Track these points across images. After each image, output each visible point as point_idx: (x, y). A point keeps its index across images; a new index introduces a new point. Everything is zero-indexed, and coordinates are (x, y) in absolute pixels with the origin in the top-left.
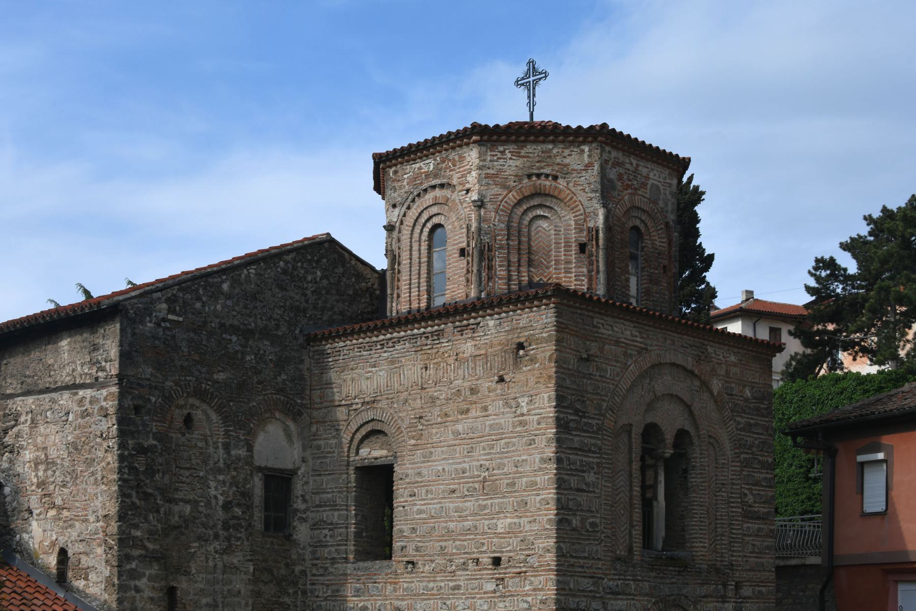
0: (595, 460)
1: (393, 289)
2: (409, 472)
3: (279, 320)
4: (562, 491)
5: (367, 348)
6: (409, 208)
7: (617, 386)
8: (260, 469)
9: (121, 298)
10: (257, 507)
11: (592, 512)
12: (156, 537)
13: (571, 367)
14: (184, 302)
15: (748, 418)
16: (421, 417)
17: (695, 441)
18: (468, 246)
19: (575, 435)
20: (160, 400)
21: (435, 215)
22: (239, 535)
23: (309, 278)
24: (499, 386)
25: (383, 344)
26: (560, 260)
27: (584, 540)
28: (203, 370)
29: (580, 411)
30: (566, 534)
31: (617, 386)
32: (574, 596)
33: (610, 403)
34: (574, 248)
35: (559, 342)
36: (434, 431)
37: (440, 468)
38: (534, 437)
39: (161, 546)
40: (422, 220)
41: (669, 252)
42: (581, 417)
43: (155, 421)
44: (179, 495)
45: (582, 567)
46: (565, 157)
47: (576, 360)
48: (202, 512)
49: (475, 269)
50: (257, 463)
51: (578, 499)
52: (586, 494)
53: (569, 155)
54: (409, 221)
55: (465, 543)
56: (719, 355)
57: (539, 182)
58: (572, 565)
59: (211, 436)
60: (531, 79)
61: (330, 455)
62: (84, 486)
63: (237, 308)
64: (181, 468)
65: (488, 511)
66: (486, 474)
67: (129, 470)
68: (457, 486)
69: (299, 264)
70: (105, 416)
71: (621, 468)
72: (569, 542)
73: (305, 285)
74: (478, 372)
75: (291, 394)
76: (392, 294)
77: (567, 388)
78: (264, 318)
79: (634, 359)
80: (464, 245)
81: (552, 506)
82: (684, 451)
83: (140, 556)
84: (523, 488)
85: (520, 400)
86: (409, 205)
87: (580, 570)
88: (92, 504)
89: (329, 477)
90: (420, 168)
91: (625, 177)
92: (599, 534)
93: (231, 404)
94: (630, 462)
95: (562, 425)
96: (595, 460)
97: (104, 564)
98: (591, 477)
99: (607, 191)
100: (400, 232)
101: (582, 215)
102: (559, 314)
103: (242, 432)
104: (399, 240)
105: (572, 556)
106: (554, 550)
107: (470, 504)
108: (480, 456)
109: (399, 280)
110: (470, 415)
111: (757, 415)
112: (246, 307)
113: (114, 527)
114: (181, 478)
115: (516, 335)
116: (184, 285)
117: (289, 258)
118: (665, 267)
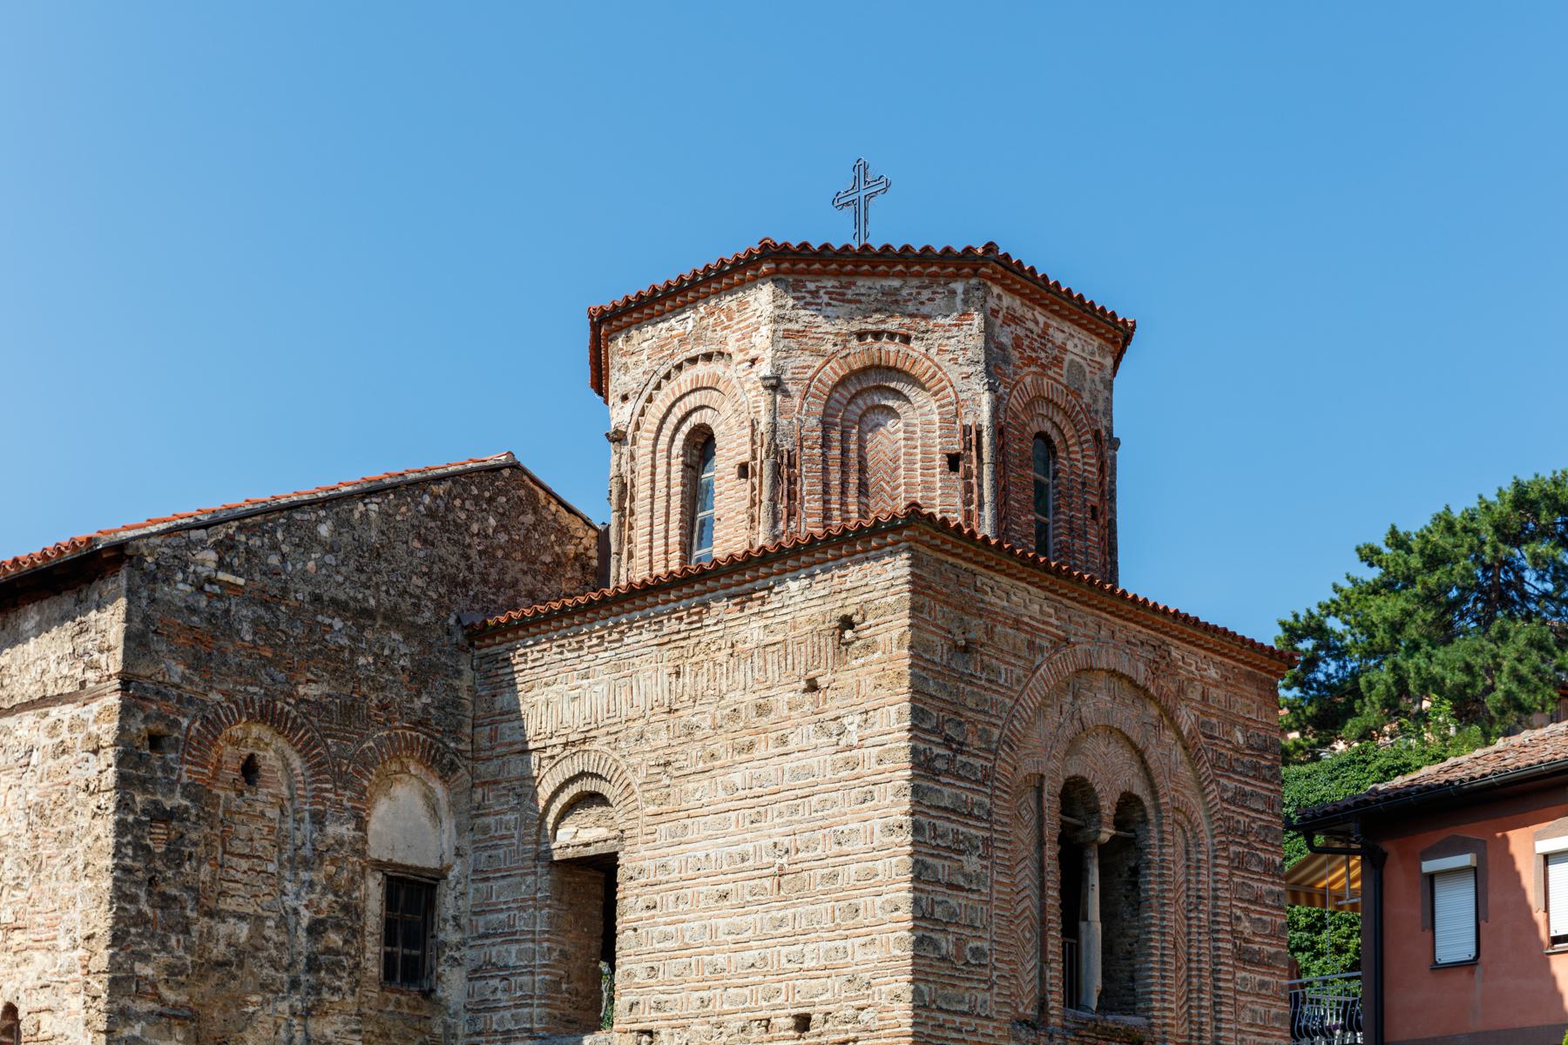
0: (981, 833)
1: (620, 543)
2: (645, 864)
3: (418, 598)
4: (922, 886)
5: (575, 645)
6: (650, 400)
7: (1017, 700)
8: (379, 865)
9: (130, 534)
10: (372, 934)
11: (976, 928)
12: (182, 978)
13: (937, 659)
14: (248, 550)
15: (1240, 781)
16: (667, 764)
17: (1151, 814)
18: (754, 458)
19: (945, 784)
20: (197, 724)
21: (696, 409)
22: (338, 983)
23: (475, 528)
24: (809, 697)
25: (602, 637)
26: (913, 484)
28: (281, 677)
29: (952, 740)
30: (931, 966)
31: (1017, 700)
33: (1006, 731)
34: (939, 461)
35: (915, 610)
36: (691, 786)
37: (701, 854)
38: (871, 787)
39: (191, 997)
40: (673, 420)
41: (1101, 484)
42: (956, 751)
43: (187, 762)
44: (228, 904)
45: (959, 1031)
46: (922, 303)
48: (270, 939)
49: (765, 496)
50: (373, 854)
52: (964, 894)
53: (929, 300)
54: (651, 422)
55: (746, 991)
56: (1191, 665)
57: (877, 346)
58: (940, 1026)
59: (291, 799)
60: (862, 194)
61: (505, 842)
62: (53, 883)
63: (343, 569)
64: (232, 854)
65: (788, 929)
66: (785, 860)
67: (134, 849)
68: (731, 886)
69: (458, 502)
70: (95, 752)
71: (1025, 853)
72: (935, 982)
73: (468, 540)
74: (770, 674)
75: (438, 731)
76: (619, 554)
77: (932, 697)
78: (392, 592)
79: (1046, 655)
80: (746, 457)
81: (905, 913)
82: (1132, 835)
83: (152, 1012)
84: (852, 882)
85: (845, 721)
86: (651, 395)
87: (954, 1035)
88: (65, 917)
89: (502, 883)
90: (670, 329)
91: (1026, 342)
93: (329, 741)
94: (1041, 844)
95: (922, 764)
96: (981, 833)
97: (81, 1027)
98: (972, 864)
99: (996, 364)
100: (634, 442)
101: (951, 404)
102: (915, 562)
103: (348, 793)
104: (633, 458)
105: (940, 1009)
106: (908, 996)
107: (755, 919)
108: (774, 829)
109: (631, 528)
110: (756, 754)
111: (1254, 777)
112: (360, 570)
113: (102, 959)
114: (232, 872)
115: (839, 604)
116: (248, 520)
117: (440, 489)
118: (1094, 509)
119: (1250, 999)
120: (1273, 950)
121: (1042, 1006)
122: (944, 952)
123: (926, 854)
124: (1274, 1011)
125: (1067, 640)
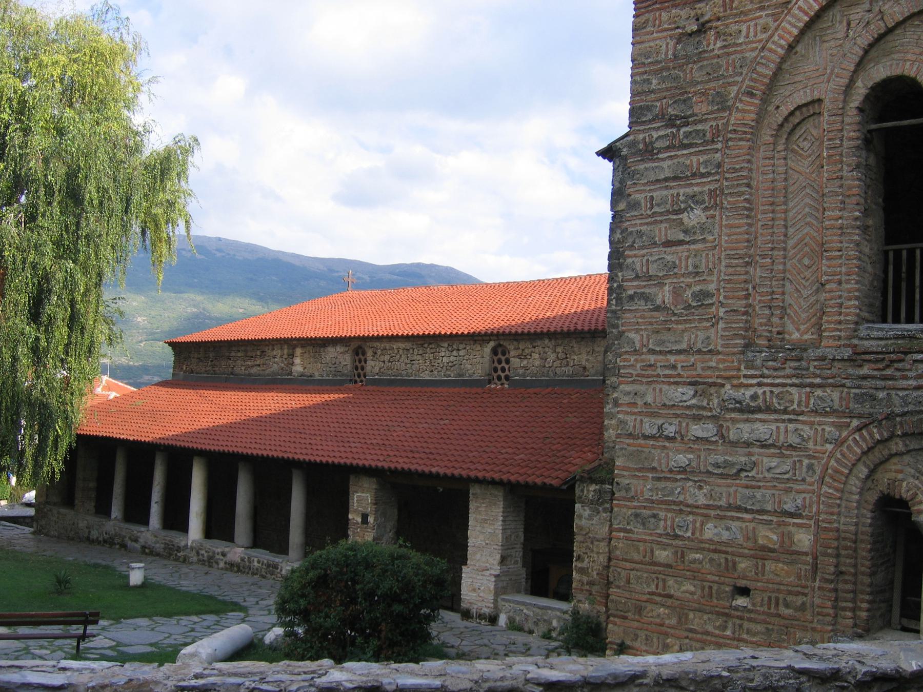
7: (763, 48)
11: (697, 273)
19: (663, 160)
27: (678, 322)
30: (643, 317)
32: (653, 415)
45: (674, 367)
47: (672, 43)
51: (669, 258)
58: (650, 366)
87: (667, 372)
92: (714, 309)
96: (706, 188)
98: (695, 217)
105: (652, 352)
121: (819, 328)
122: (659, 302)
123: (641, 224)
125: (105, 139)
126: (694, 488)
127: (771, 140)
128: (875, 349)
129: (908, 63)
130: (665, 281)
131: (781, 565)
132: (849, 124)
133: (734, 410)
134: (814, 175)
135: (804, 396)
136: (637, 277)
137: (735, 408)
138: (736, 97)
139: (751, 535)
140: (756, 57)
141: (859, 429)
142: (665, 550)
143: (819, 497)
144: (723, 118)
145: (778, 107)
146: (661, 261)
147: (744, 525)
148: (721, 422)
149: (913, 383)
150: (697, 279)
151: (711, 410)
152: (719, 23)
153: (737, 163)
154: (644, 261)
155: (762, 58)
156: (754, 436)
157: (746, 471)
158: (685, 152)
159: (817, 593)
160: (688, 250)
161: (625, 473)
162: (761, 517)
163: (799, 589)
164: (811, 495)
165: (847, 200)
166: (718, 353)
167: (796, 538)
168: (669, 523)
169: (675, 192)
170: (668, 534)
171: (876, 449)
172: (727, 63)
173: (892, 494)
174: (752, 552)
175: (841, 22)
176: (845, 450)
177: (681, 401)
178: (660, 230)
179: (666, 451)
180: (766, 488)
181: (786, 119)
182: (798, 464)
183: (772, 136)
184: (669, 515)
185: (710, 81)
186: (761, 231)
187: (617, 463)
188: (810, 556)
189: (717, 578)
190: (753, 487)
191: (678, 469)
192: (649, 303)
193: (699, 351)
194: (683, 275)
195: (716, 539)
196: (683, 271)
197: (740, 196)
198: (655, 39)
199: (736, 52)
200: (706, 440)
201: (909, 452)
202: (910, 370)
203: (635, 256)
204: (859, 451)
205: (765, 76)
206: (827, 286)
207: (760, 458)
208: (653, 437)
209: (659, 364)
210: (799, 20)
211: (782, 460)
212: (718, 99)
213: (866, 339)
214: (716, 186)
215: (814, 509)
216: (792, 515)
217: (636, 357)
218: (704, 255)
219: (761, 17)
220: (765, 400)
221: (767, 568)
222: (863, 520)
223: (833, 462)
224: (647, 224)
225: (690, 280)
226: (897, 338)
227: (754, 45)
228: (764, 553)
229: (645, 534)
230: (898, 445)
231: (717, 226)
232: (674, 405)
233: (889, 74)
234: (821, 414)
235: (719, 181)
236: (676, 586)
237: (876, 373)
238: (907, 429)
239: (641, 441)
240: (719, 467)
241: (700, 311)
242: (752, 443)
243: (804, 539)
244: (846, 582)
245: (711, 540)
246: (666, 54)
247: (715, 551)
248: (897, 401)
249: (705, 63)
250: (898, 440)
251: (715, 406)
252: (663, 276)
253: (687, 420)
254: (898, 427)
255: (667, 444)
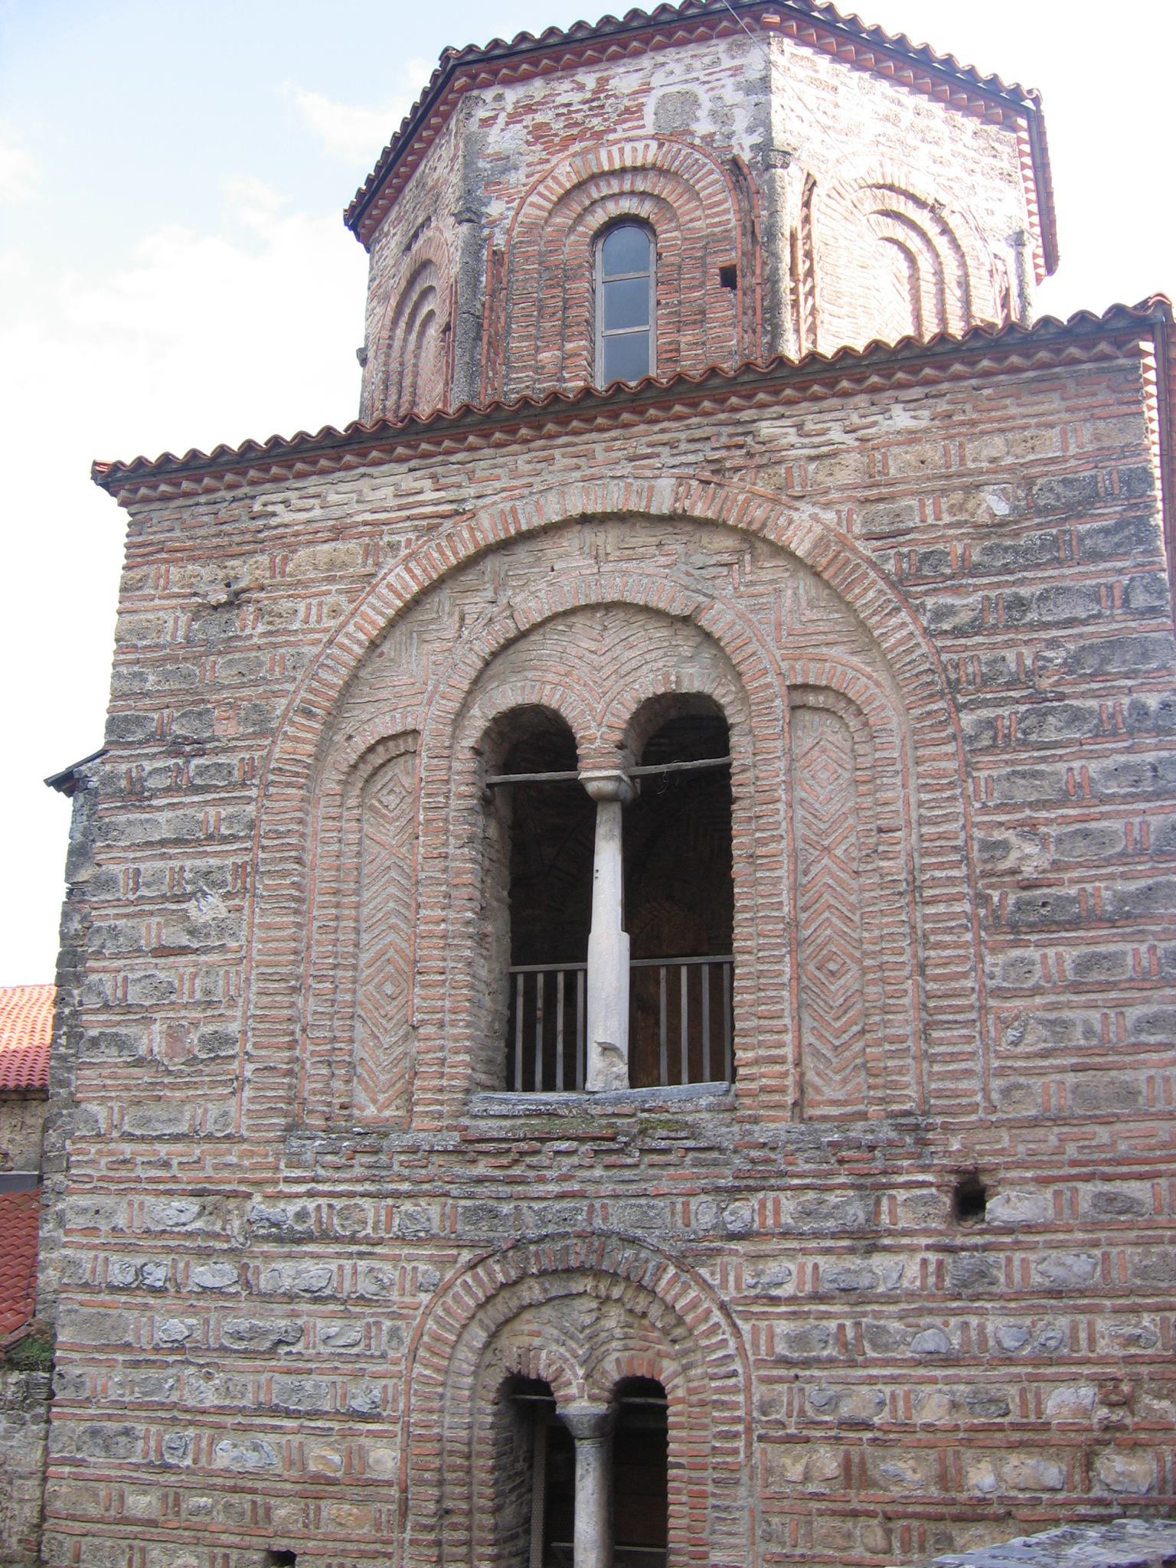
7: (330, 642)
19: (160, 809)
27: (174, 1087)
32: (126, 1248)
33: (303, 694)
45: (166, 1165)
47: (184, 619)
51: (162, 975)
58: (125, 1162)
79: (403, 552)
92: (235, 1065)
96: (229, 861)
98: (209, 909)
105: (129, 1137)
119: (1038, 1000)
120: (1132, 886)
122: (142, 1051)
123: (117, 916)
124: (1133, 1013)
126: (198, 1378)
127: (338, 788)
128: (495, 1134)
129: (548, 687)
130: (155, 1016)
131: (347, 1507)
132: (459, 773)
133: (266, 1238)
134: (404, 850)
135: (383, 1212)
136: (107, 1007)
137: (270, 1235)
138: (285, 715)
139: (295, 1456)
140: (318, 656)
141: (472, 1266)
142: (145, 1493)
143: (409, 1383)
144: (262, 747)
145: (350, 737)
146: (148, 981)
147: (284, 1439)
148: (245, 1260)
149: (554, 1188)
150: (209, 1013)
151: (228, 1240)
152: (263, 595)
153: (281, 822)
154: (120, 979)
155: (328, 656)
156: (302, 1283)
157: (288, 1344)
158: (196, 799)
159: (409, 1550)
160: (196, 964)
161: (76, 1356)
162: (313, 1424)
163: (378, 1546)
164: (395, 1380)
165: (454, 893)
166: (243, 1140)
167: (373, 1457)
168: (152, 1444)
169: (176, 864)
170: (150, 1464)
171: (499, 1299)
172: (273, 659)
173: (524, 1372)
174: (298, 1487)
175: (450, 614)
176: (450, 1301)
177: (177, 1225)
178: (149, 927)
179: (148, 1314)
180: (322, 1372)
181: (362, 758)
182: (373, 1329)
183: (340, 782)
184: (153, 1429)
185: (243, 685)
186: (317, 937)
187: (60, 1338)
188: (396, 1488)
189: (236, 1539)
190: (298, 1372)
191: (169, 1345)
192: (125, 1052)
193: (209, 1137)
194: (185, 1006)
195: (236, 1467)
196: (185, 999)
197: (284, 877)
198: (155, 609)
199: (287, 644)
200: (219, 1292)
201: (550, 1300)
202: (550, 1167)
203: (105, 970)
204: (472, 1303)
205: (332, 687)
206: (421, 1031)
207: (312, 1319)
208: (125, 1289)
209: (139, 1159)
210: (388, 604)
211: (346, 1321)
212: (255, 717)
213: (482, 1117)
214: (246, 858)
215: (401, 1406)
216: (364, 1417)
217: (99, 1146)
218: (222, 973)
219: (329, 593)
220: (319, 1221)
221: (324, 1514)
222: (481, 1418)
223: (431, 1324)
224: (127, 916)
225: (195, 1014)
226: (529, 1115)
227: (317, 636)
228: (319, 1487)
229: (110, 1466)
230: (532, 1291)
231: (244, 925)
232: (164, 1231)
233: (520, 701)
234: (410, 1243)
235: (251, 850)
236: (165, 1559)
237: (497, 1173)
238: (547, 1264)
239: (105, 1297)
240: (242, 1339)
241: (213, 1067)
242: (297, 1296)
243: (385, 1459)
244: (454, 1527)
245: (227, 1470)
246: (174, 636)
247: (234, 1490)
248: (530, 1218)
249: (237, 656)
250: (532, 1282)
251: (236, 1231)
252: (151, 1006)
253: (186, 1258)
254: (533, 1261)
255: (151, 1301)
